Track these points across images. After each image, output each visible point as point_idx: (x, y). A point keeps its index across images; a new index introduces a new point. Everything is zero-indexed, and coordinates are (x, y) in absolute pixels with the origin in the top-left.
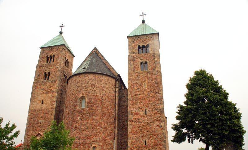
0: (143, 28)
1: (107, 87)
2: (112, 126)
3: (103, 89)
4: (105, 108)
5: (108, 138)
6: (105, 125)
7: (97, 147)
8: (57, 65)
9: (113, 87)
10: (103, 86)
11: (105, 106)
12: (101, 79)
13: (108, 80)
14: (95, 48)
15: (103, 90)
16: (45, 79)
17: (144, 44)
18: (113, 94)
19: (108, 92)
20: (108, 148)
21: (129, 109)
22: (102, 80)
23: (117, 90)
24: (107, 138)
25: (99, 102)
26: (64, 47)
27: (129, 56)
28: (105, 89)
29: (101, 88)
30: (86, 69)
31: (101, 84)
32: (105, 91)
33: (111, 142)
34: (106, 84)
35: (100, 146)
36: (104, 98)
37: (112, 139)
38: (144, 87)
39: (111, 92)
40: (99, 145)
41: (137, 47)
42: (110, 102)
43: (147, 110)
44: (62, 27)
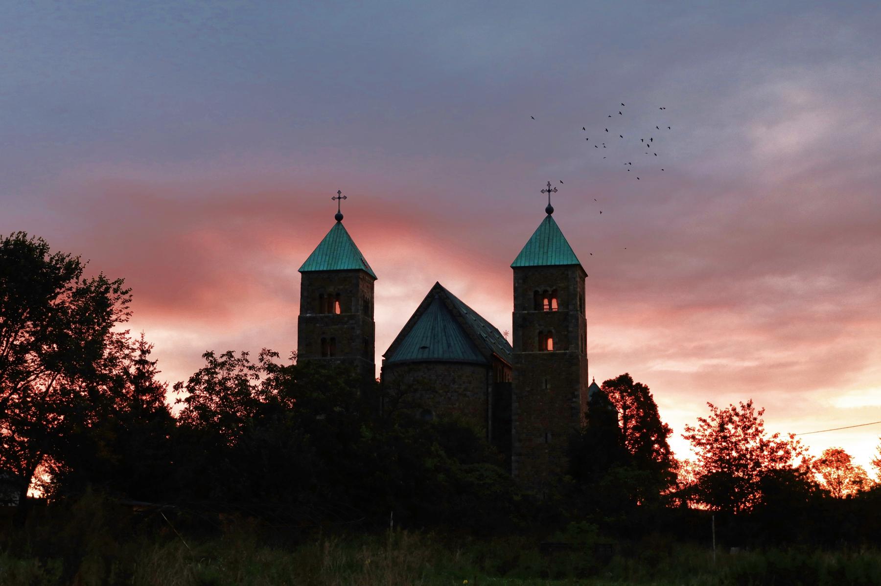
0: (546, 240)
8: (351, 322)
14: (438, 283)
16: (324, 354)
17: (548, 289)
21: (514, 431)
23: (490, 390)
27: (514, 314)
30: (427, 350)
38: (544, 387)
41: (531, 294)
43: (549, 435)
44: (339, 198)
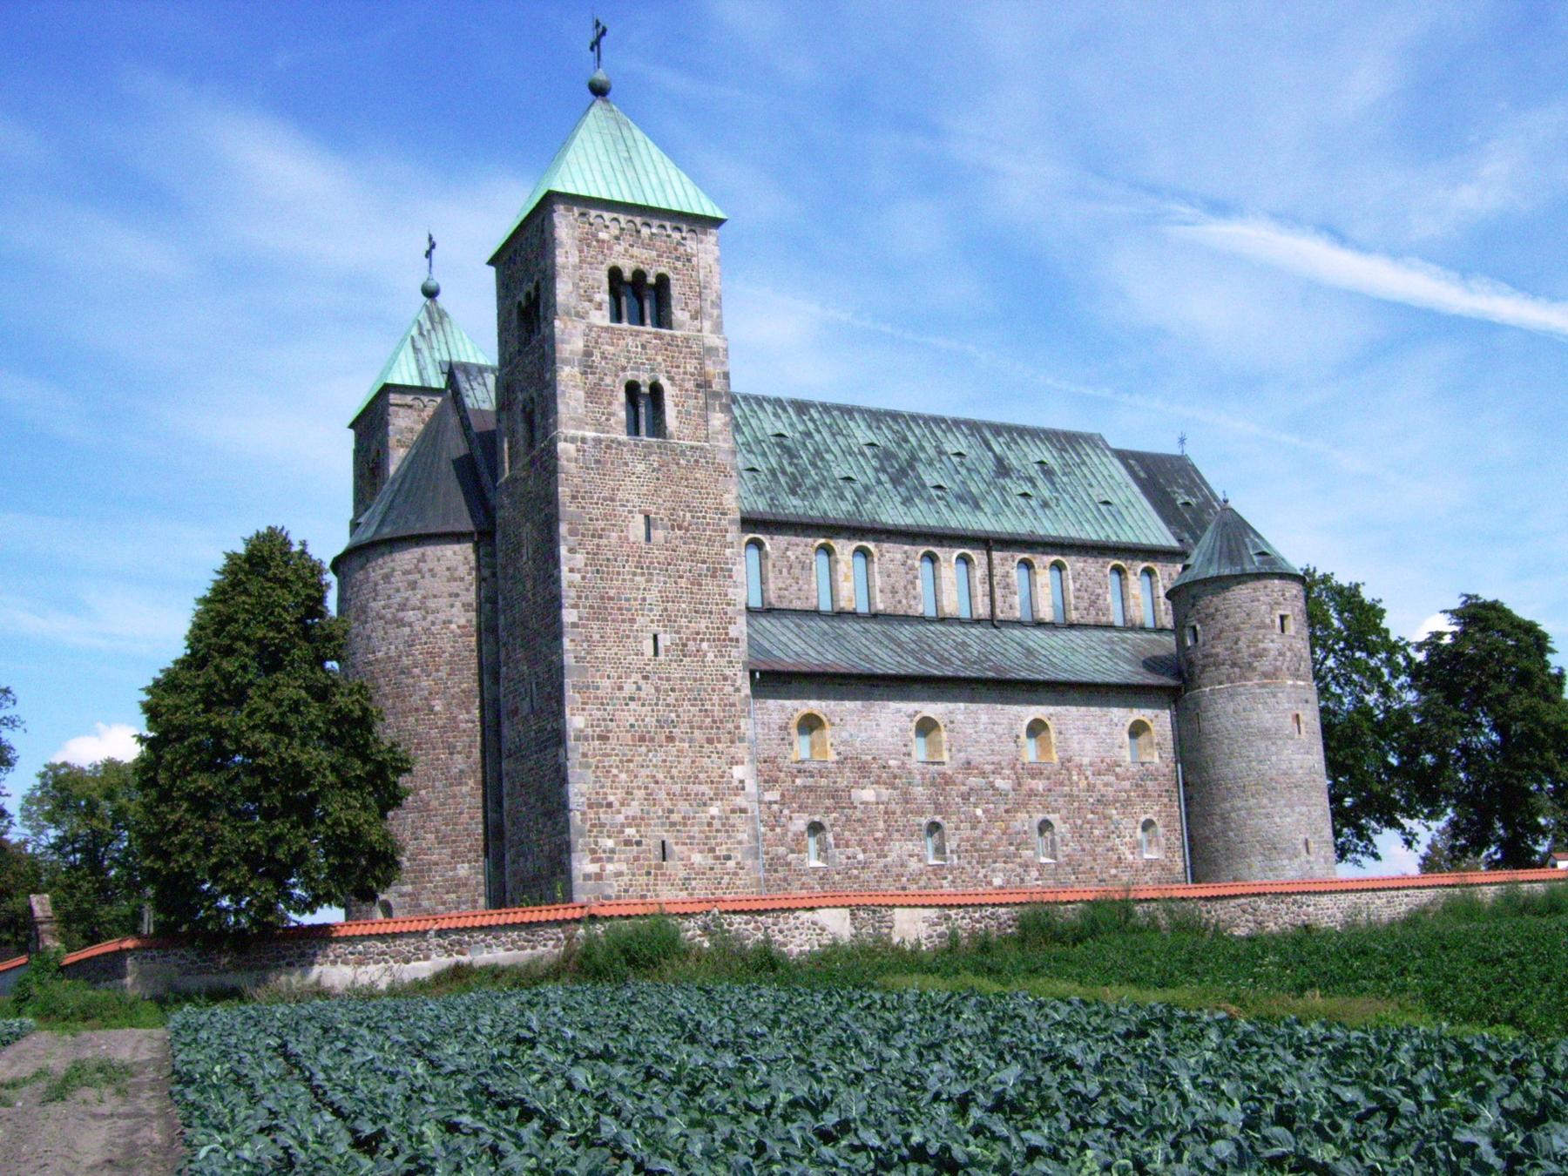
1: (415, 601)
2: (464, 789)
3: (401, 615)
4: (417, 710)
5: (440, 854)
6: (423, 792)
7: (392, 903)
9: (455, 587)
10: (397, 599)
11: (416, 700)
12: (386, 570)
13: (423, 559)
15: (401, 623)
18: (463, 622)
19: (426, 624)
20: (444, 903)
22: (393, 570)
24: (435, 858)
25: (387, 690)
26: (394, 398)
28: (410, 615)
29: (389, 616)
31: (389, 597)
32: (410, 625)
33: (463, 870)
34: (413, 586)
35: (402, 895)
36: (406, 661)
37: (472, 855)
39: (442, 616)
40: (402, 895)
42: (443, 674)
